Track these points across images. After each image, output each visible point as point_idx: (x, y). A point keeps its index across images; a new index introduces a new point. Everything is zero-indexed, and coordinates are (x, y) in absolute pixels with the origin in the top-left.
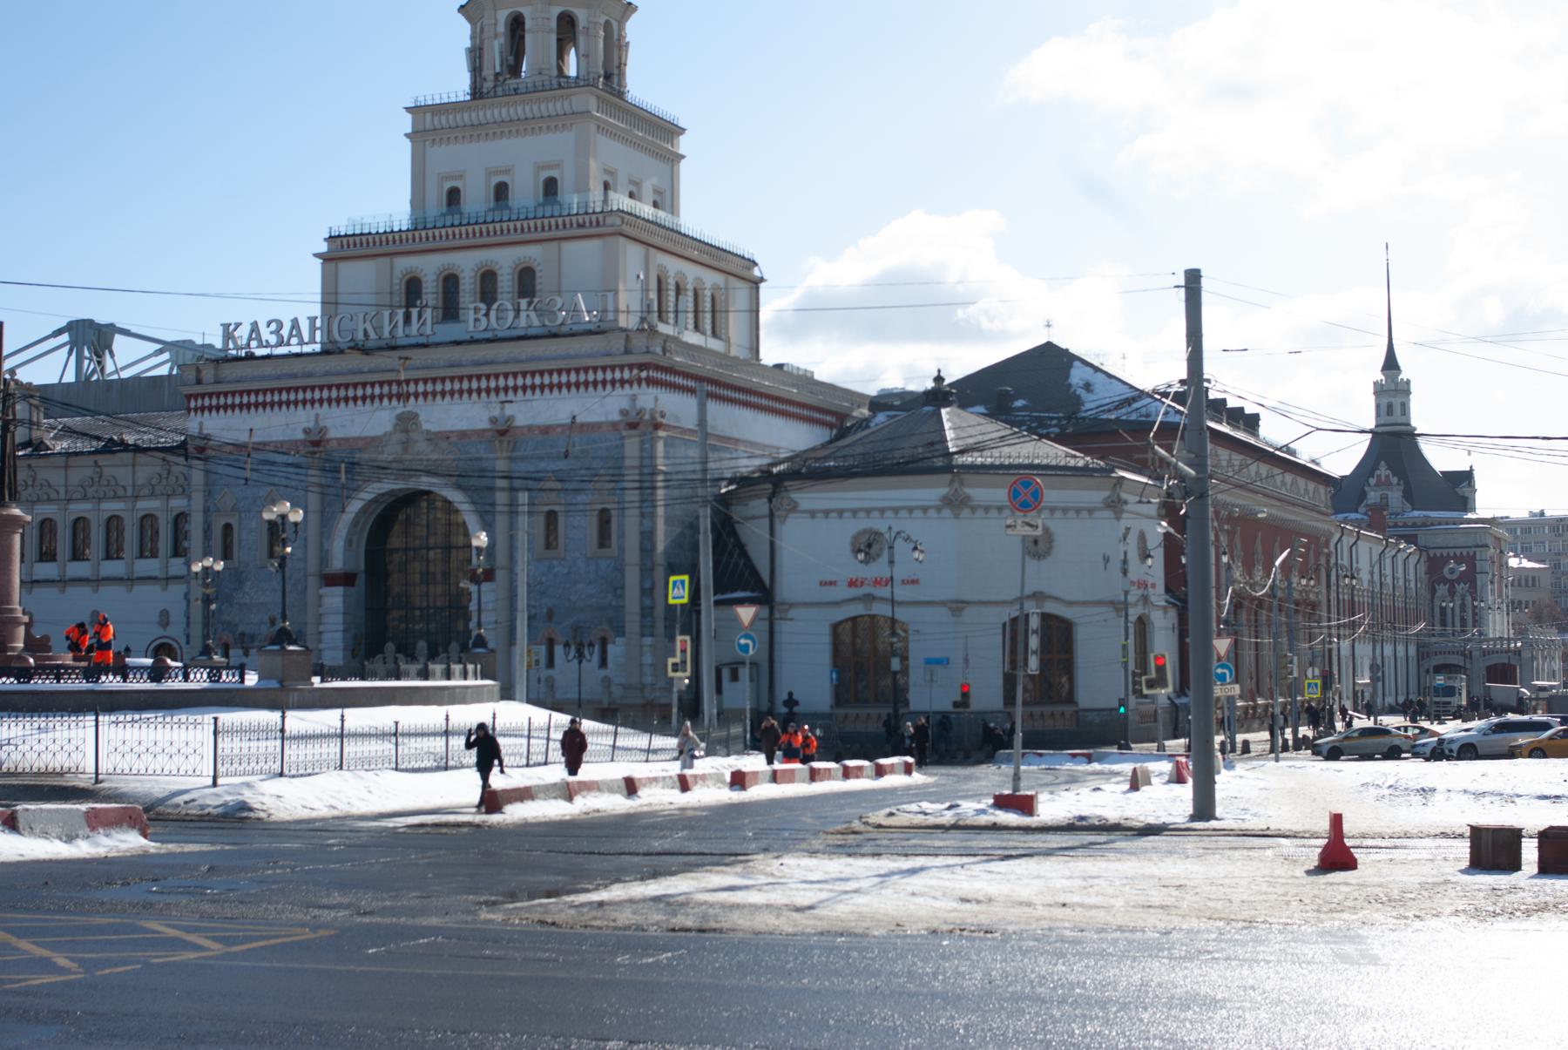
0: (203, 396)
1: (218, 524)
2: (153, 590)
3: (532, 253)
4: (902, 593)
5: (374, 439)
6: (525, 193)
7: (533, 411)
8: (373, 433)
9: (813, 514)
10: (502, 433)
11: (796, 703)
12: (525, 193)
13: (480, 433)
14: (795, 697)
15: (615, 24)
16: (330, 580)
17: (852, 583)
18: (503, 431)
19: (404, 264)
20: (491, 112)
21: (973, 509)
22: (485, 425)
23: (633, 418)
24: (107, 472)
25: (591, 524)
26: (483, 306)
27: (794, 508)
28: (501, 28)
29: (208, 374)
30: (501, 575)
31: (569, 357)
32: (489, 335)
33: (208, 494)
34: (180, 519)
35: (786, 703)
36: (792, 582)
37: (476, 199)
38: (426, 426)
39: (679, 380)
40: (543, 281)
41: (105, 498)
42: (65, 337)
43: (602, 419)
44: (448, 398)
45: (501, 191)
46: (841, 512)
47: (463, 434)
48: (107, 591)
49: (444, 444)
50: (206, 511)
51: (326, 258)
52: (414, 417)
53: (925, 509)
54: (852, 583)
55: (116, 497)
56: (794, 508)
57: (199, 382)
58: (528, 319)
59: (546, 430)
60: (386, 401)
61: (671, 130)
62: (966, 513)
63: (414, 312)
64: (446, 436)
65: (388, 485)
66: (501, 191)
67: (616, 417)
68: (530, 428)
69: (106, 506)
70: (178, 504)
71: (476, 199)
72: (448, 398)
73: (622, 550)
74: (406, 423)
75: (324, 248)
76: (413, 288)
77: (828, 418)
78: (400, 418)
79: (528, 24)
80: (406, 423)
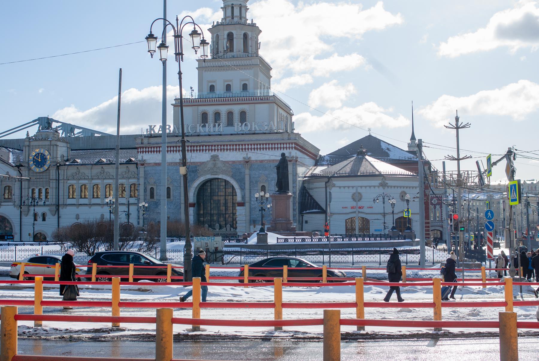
2: (98, 208)
4: (366, 210)
5: (203, 163)
6: (236, 88)
7: (255, 156)
8: (203, 161)
9: (340, 187)
10: (247, 162)
12: (236, 88)
13: (240, 162)
17: (352, 208)
18: (247, 162)
19: (202, 109)
20: (216, 63)
21: (388, 187)
24: (81, 171)
26: (240, 124)
27: (334, 186)
28: (226, 37)
29: (146, 141)
30: (247, 205)
31: (269, 140)
33: (145, 178)
36: (334, 207)
37: (220, 90)
38: (221, 159)
41: (106, 179)
44: (229, 151)
45: (228, 88)
46: (349, 187)
47: (234, 162)
49: (227, 165)
50: (145, 183)
52: (217, 156)
53: (374, 187)
54: (352, 208)
55: (110, 179)
56: (334, 186)
58: (243, 128)
59: (262, 161)
60: (207, 151)
62: (386, 187)
63: (217, 124)
65: (209, 177)
66: (228, 88)
68: (256, 161)
69: (81, 181)
71: (220, 90)
72: (229, 151)
74: (215, 158)
75: (174, 102)
76: (204, 116)
78: (212, 156)
79: (235, 36)
80: (215, 158)
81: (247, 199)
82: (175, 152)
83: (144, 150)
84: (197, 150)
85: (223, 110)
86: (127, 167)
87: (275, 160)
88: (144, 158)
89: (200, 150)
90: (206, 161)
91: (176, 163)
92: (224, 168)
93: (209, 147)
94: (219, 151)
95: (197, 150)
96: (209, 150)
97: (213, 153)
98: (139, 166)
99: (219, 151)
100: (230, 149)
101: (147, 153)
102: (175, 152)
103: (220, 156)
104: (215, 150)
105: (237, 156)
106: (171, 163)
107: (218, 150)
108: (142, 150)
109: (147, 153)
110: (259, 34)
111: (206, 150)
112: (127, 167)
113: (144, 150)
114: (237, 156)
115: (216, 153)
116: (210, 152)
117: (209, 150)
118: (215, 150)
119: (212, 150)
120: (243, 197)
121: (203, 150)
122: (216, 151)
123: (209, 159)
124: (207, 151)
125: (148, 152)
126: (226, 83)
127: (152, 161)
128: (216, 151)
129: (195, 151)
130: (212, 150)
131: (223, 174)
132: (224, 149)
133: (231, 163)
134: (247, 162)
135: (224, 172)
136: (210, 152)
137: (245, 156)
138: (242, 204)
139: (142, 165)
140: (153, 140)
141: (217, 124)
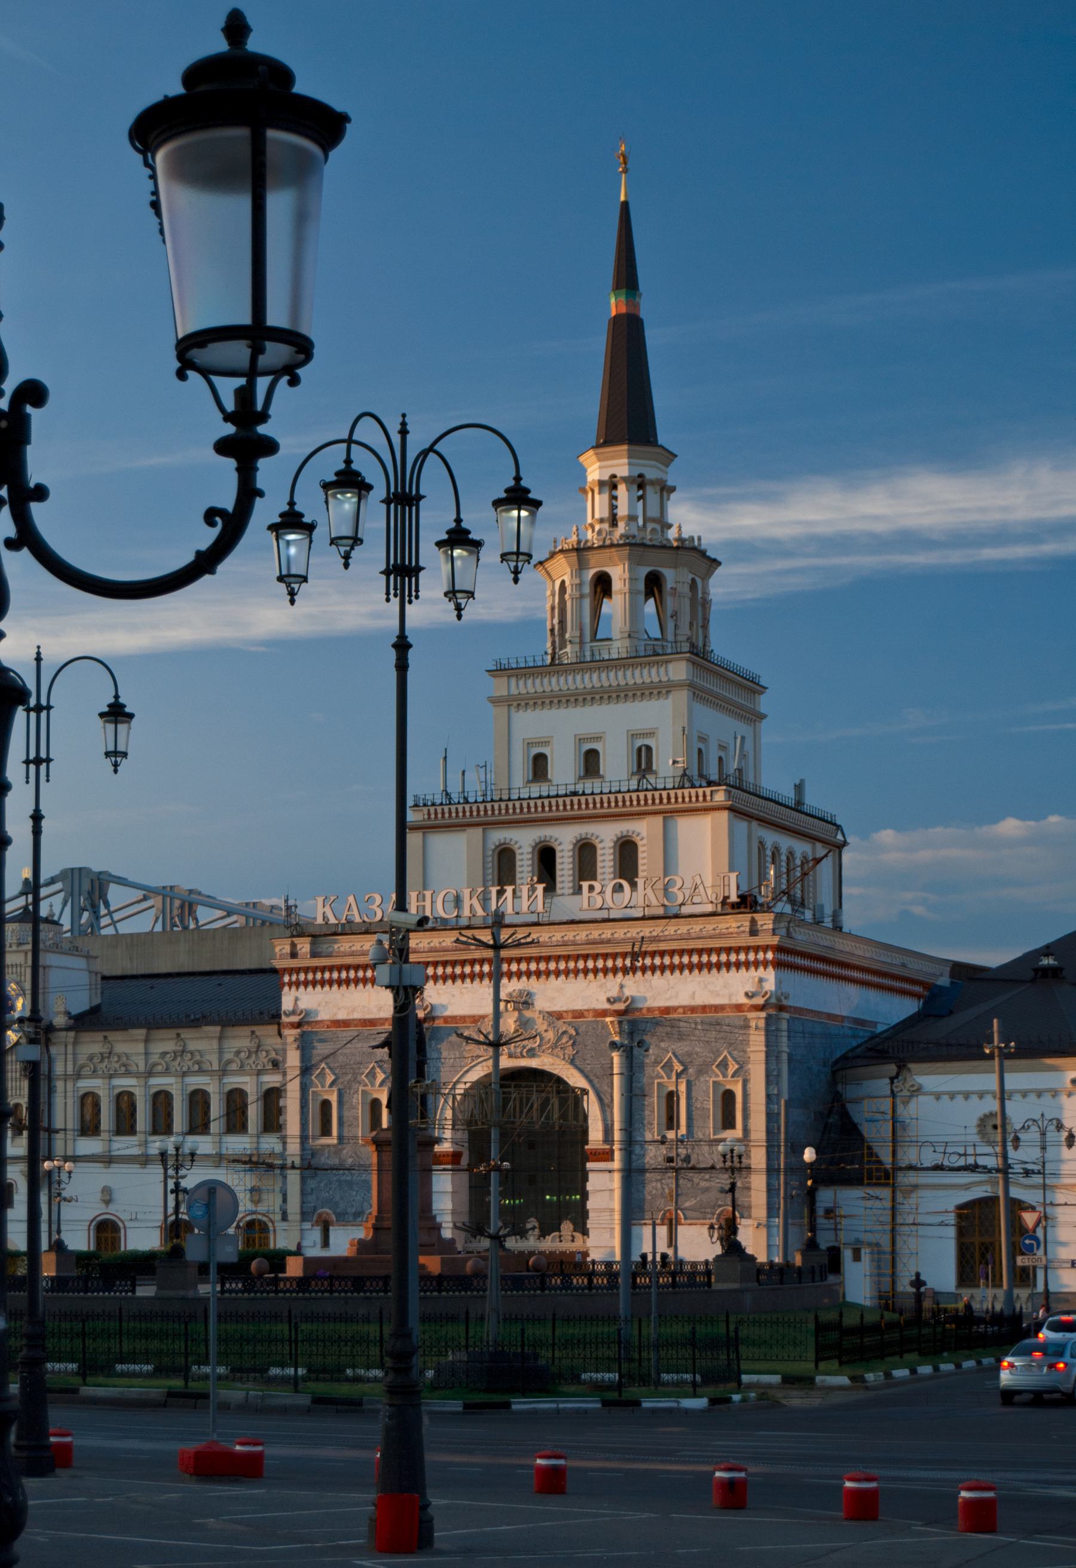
0: (298, 970)
9: (938, 1096)
11: (924, 1283)
14: (922, 1278)
15: (699, 581)
19: (498, 836)
25: (710, 1105)
27: (918, 1091)
32: (604, 914)
34: (272, 1098)
35: (912, 1284)
39: (799, 961)
40: (648, 860)
42: (59, 886)
46: (967, 1095)
47: (579, 1014)
56: (918, 1091)
57: (294, 955)
59: (667, 1010)
61: (753, 686)
64: (559, 1015)
70: (272, 1080)
73: (746, 1130)
77: (917, 989)
83: (302, 977)
85: (564, 839)
86: (253, 1032)
105: (587, 994)
108: (294, 978)
110: (709, 573)
112: (253, 1032)
120: (608, 1131)
127: (324, 1015)
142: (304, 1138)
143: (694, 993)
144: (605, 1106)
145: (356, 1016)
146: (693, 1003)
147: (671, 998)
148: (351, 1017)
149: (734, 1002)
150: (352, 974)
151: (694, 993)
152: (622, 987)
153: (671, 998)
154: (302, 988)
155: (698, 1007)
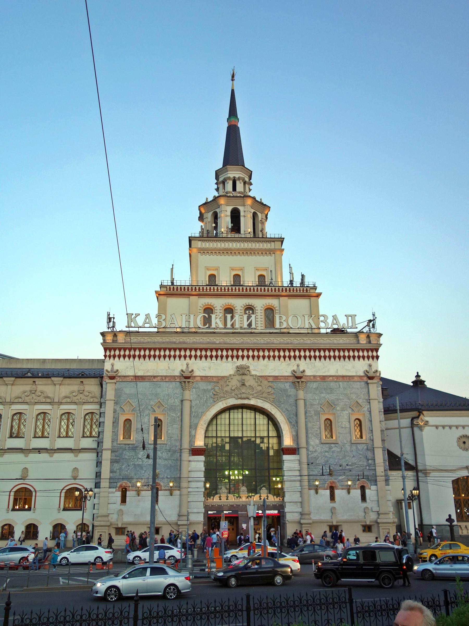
1: (122, 419)
3: (273, 302)
5: (223, 377)
6: (250, 280)
8: (222, 375)
12: (250, 280)
16: (196, 452)
18: (298, 379)
22: (290, 374)
23: (371, 374)
28: (229, 213)
30: (303, 452)
37: (225, 280)
38: (253, 373)
43: (354, 374)
44: (266, 359)
48: (34, 457)
49: (265, 382)
50: (115, 411)
51: (158, 294)
56: (427, 423)
60: (230, 359)
64: (266, 377)
67: (362, 374)
71: (225, 280)
72: (266, 359)
74: (242, 371)
76: (209, 310)
78: (239, 369)
79: (242, 214)
80: (242, 371)
81: (303, 443)
82: (172, 359)
83: (117, 353)
84: (211, 357)
87: (347, 376)
88: (115, 368)
89: (217, 357)
90: (227, 374)
91: (174, 376)
92: (260, 388)
93: (233, 352)
94: (251, 359)
95: (211, 357)
96: (232, 357)
97: (240, 362)
98: (106, 380)
99: (251, 359)
100: (269, 357)
101: (122, 358)
102: (172, 359)
103: (251, 368)
104: (243, 357)
106: (166, 377)
107: (248, 357)
109: (122, 358)
111: (227, 357)
113: (117, 353)
114: (282, 368)
115: (245, 362)
116: (235, 359)
117: (232, 357)
118: (243, 357)
119: (238, 357)
121: (222, 357)
122: (245, 359)
123: (232, 372)
124: (230, 359)
125: (124, 356)
126: (234, 273)
128: (245, 359)
129: (209, 359)
130: (238, 357)
131: (256, 398)
132: (258, 357)
133: (271, 379)
134: (298, 379)
135: (259, 395)
136: (235, 359)
137: (295, 368)
138: (292, 451)
139: (112, 378)
140: (134, 339)
141: (245, 317)
142: (114, 440)
143: (337, 370)
144: (294, 425)
145: (149, 374)
146: (337, 375)
147: (325, 372)
148: (146, 375)
149: (358, 374)
150: (147, 353)
151: (337, 370)
152: (298, 366)
153: (325, 372)
154: (117, 359)
155: (340, 376)
